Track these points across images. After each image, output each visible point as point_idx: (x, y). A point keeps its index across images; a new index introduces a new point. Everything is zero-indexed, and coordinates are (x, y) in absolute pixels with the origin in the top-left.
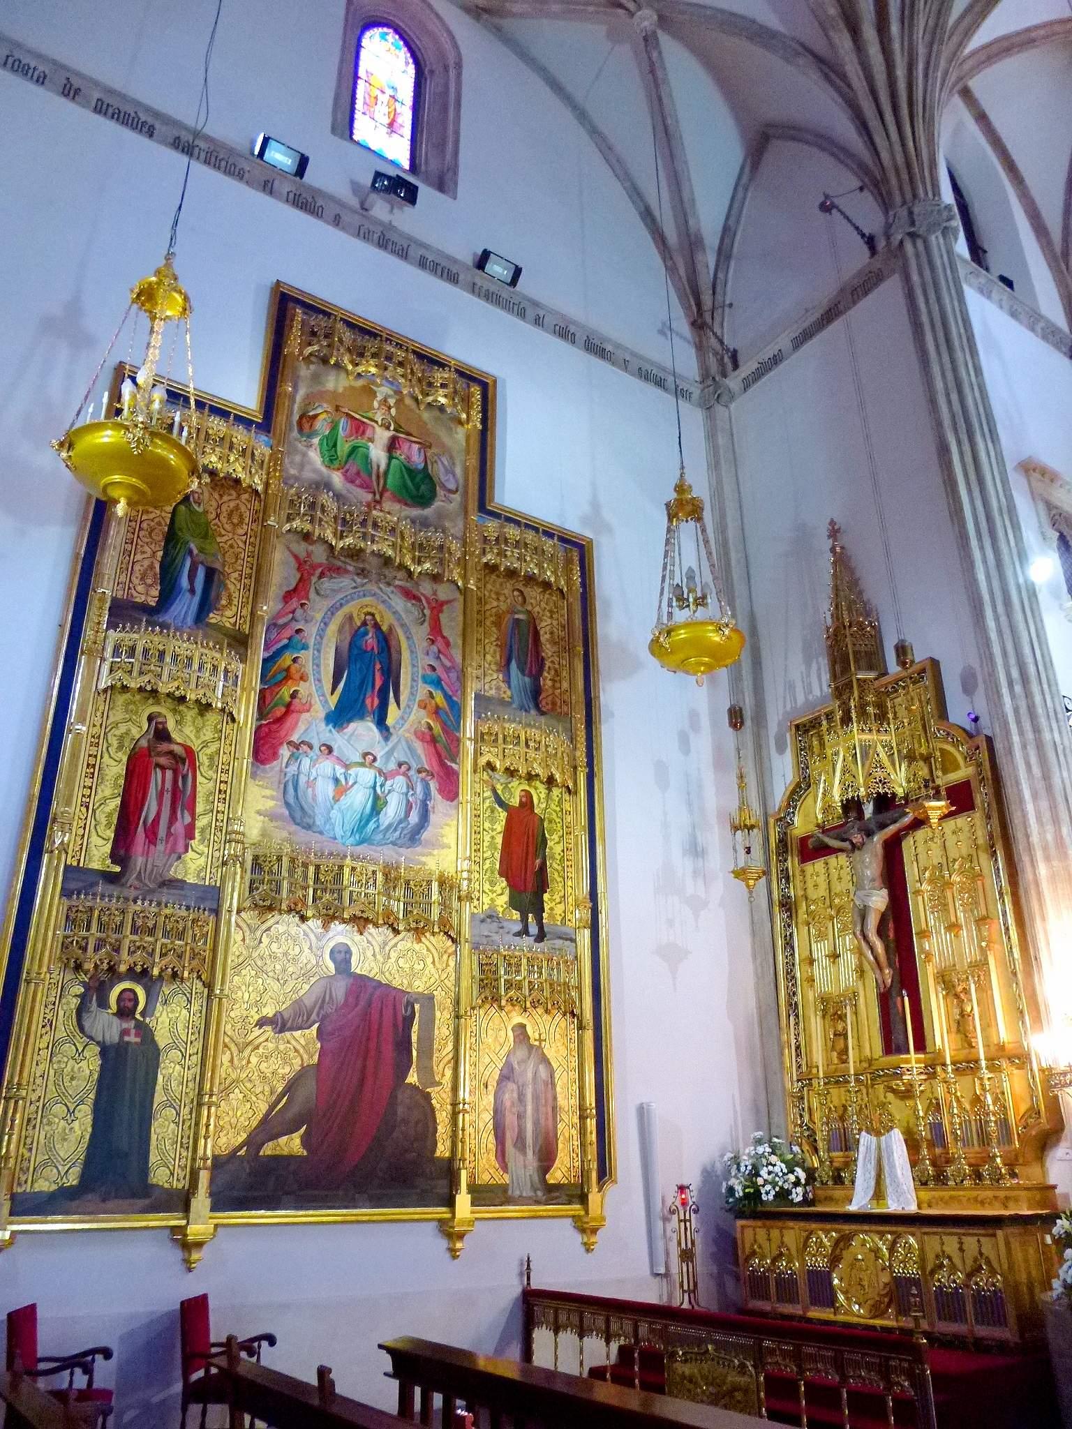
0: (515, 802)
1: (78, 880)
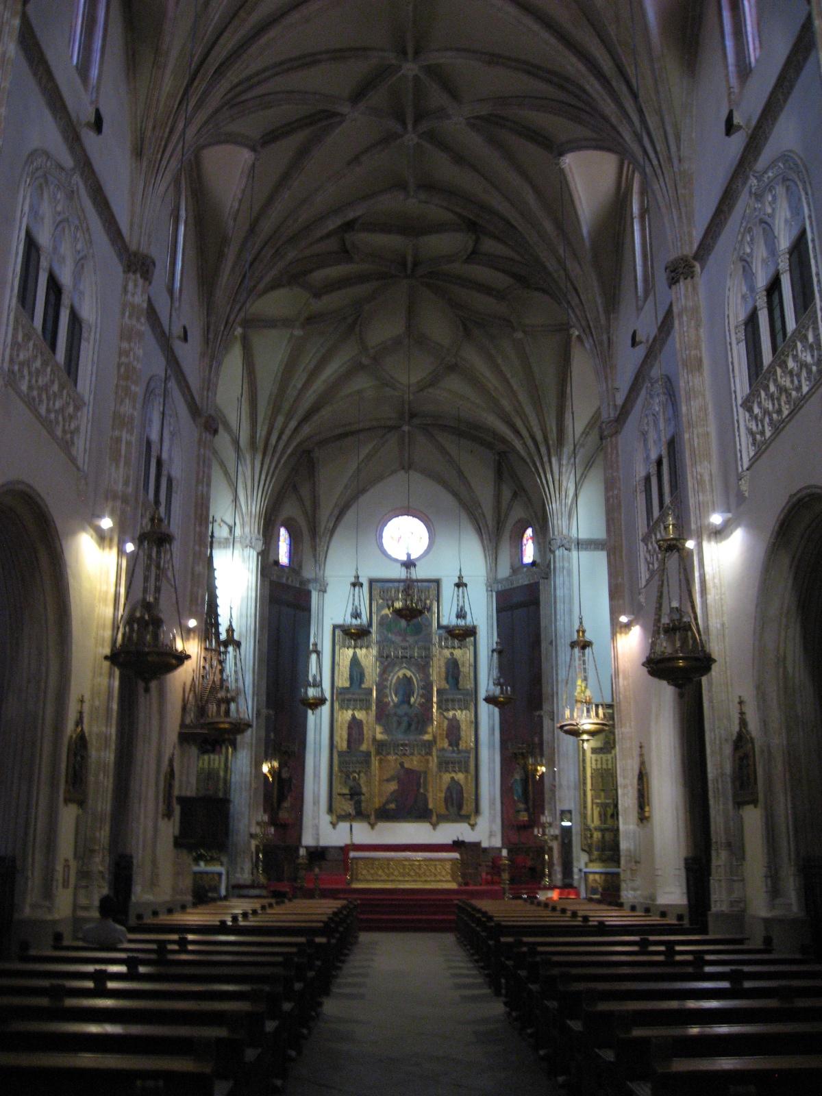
1: (341, 754)
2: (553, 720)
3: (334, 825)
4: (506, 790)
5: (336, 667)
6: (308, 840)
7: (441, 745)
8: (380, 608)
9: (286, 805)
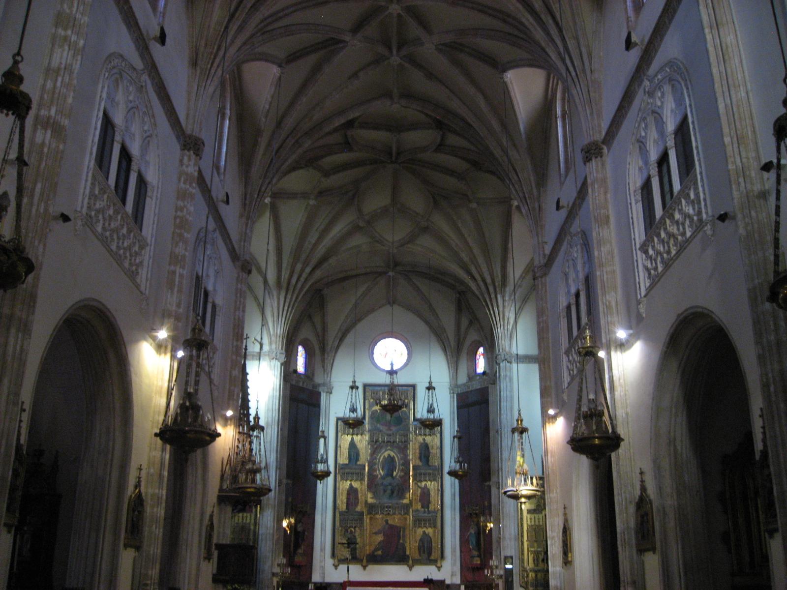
0: (423, 486)
1: (341, 514)
2: (498, 488)
3: (336, 567)
4: (464, 541)
5: (339, 449)
6: (316, 578)
7: (416, 508)
8: (371, 406)
9: (300, 551)
